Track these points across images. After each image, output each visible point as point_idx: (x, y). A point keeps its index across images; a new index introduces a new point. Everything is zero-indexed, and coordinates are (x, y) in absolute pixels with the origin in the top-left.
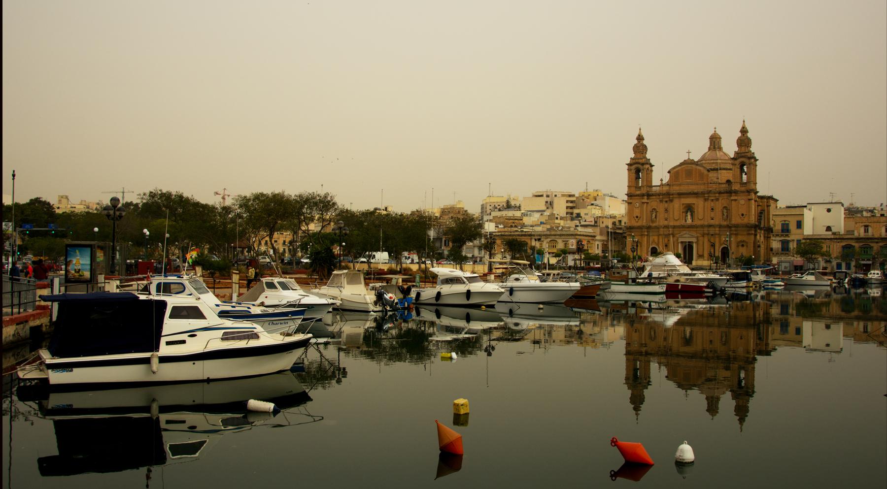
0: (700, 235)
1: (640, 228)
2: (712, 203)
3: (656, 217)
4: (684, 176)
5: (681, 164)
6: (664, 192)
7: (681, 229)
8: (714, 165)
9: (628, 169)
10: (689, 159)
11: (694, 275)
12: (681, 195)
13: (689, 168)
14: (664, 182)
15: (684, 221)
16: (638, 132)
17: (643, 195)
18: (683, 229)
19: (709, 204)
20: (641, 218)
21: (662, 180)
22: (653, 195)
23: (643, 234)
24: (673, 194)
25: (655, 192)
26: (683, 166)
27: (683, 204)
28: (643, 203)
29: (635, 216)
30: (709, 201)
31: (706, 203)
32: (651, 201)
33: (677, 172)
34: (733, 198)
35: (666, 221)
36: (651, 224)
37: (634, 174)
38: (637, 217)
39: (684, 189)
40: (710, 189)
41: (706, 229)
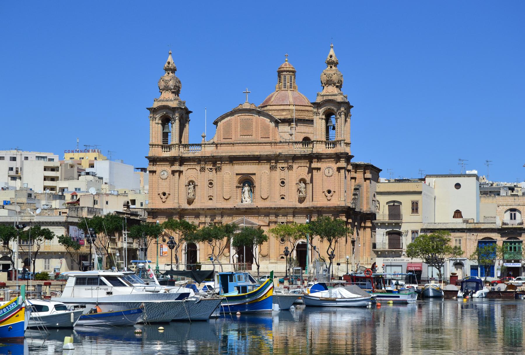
2: (283, 173)
8: (284, 113)
11: (399, 297)
12: (233, 160)
15: (239, 200)
19: (278, 174)
20: (171, 197)
27: (237, 174)
30: (278, 169)
34: (314, 165)
38: (164, 194)
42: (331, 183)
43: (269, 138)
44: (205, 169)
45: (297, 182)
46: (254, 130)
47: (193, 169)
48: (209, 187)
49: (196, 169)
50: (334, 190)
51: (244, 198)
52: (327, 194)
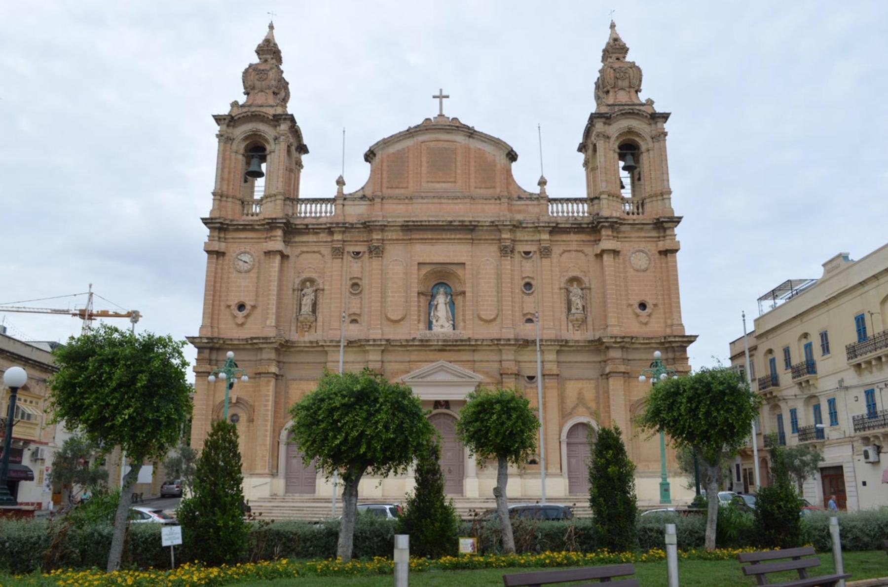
0: (489, 380)
1: (253, 345)
2: (527, 265)
3: (314, 311)
4: (424, 169)
5: (411, 133)
6: (350, 220)
7: (414, 357)
9: (219, 136)
10: (441, 115)
13: (441, 145)
14: (347, 190)
15: (422, 326)
16: (266, 34)
17: (271, 225)
18: (423, 356)
20: (258, 313)
21: (340, 182)
22: (306, 229)
23: (262, 369)
24: (383, 228)
25: (314, 221)
26: (421, 138)
27: (419, 264)
28: (268, 253)
29: (234, 301)
30: (516, 255)
31: (507, 263)
32: (297, 251)
33: (400, 158)
34: (607, 244)
35: (353, 327)
36: (294, 337)
37: (240, 157)
39: (424, 212)
40: (520, 217)
41: (509, 355)
42: (646, 285)
43: (494, 187)
44: (343, 253)
45: (562, 285)
46: (459, 171)
47: (314, 252)
48: (351, 293)
49: (321, 254)
50: (655, 302)
51: (437, 321)
52: (639, 311)
